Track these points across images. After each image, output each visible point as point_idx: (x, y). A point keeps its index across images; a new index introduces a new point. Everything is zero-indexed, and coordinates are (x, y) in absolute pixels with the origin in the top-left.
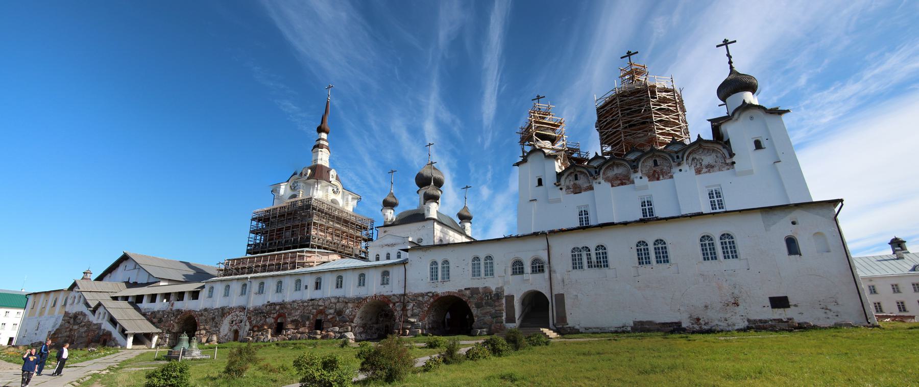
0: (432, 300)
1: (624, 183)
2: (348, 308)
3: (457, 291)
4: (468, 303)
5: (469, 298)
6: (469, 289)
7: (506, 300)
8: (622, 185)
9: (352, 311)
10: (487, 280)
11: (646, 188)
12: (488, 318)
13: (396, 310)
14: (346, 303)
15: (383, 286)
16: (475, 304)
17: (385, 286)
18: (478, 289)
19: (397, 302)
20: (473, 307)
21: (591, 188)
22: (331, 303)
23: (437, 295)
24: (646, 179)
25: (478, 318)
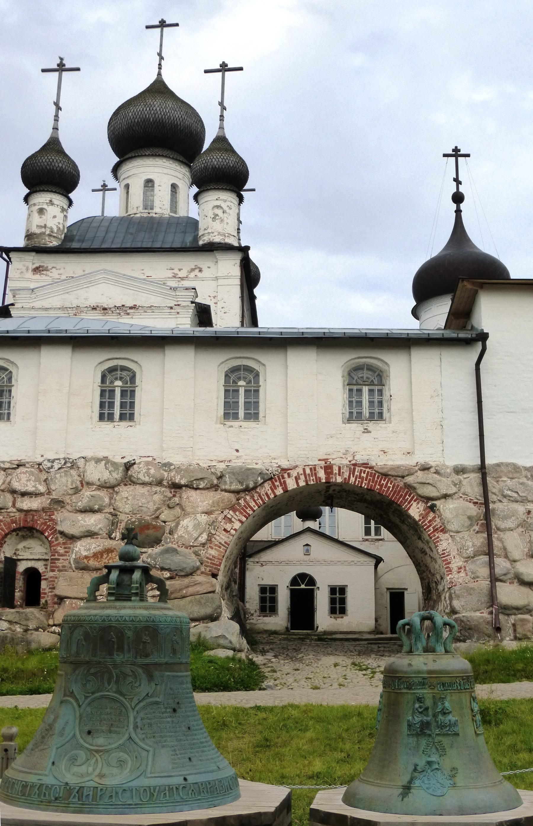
2: (186, 514)
9: (212, 524)
14: (176, 487)
15: (356, 427)
17: (371, 426)
22: (86, 484)
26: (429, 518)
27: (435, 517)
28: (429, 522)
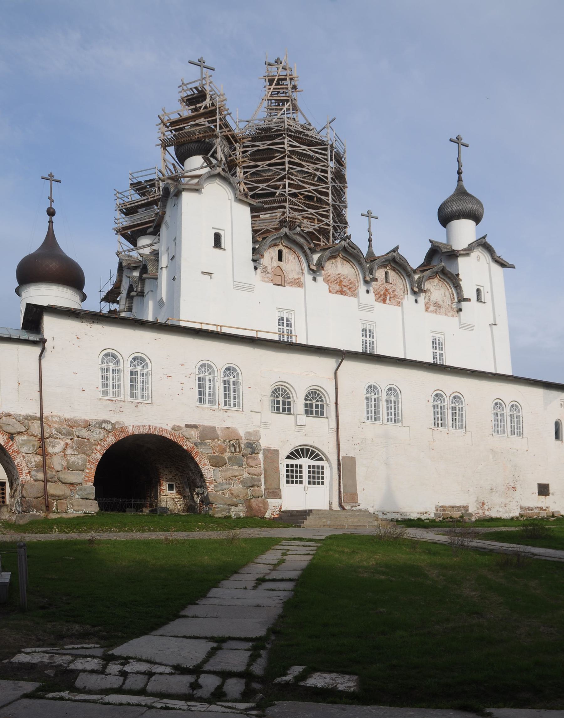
0: (111, 440)
1: (344, 292)
3: (169, 428)
4: (193, 454)
5: (196, 444)
6: (195, 427)
7: (265, 457)
10: (230, 413)
11: (369, 308)
12: (237, 487)
13: (18, 452)
16: (210, 458)
18: (213, 429)
19: (19, 433)
20: (205, 464)
21: (298, 283)
23: (122, 430)
24: (372, 295)
25: (216, 486)
26: (10, 445)
27: (13, 444)
28: (9, 447)
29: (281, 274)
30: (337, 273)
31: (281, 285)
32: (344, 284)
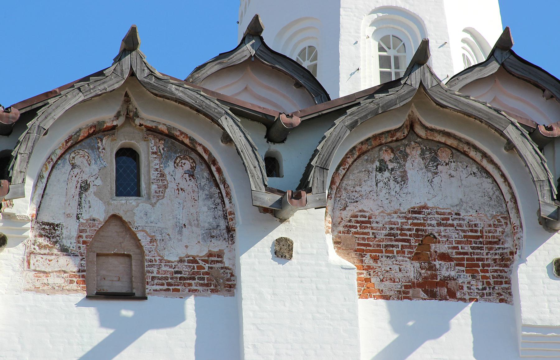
1: (444, 282)
8: (432, 295)
29: (128, 247)
30: (405, 208)
31: (128, 296)
32: (443, 248)
